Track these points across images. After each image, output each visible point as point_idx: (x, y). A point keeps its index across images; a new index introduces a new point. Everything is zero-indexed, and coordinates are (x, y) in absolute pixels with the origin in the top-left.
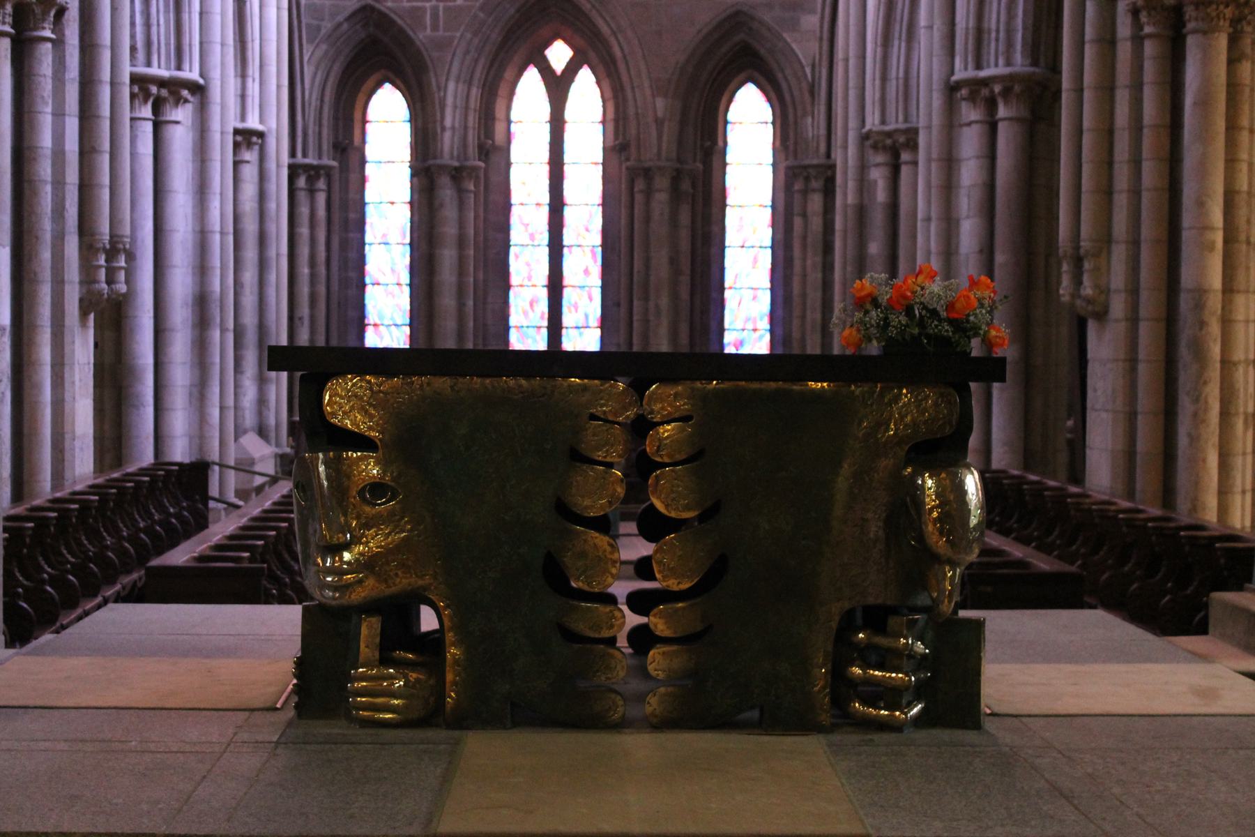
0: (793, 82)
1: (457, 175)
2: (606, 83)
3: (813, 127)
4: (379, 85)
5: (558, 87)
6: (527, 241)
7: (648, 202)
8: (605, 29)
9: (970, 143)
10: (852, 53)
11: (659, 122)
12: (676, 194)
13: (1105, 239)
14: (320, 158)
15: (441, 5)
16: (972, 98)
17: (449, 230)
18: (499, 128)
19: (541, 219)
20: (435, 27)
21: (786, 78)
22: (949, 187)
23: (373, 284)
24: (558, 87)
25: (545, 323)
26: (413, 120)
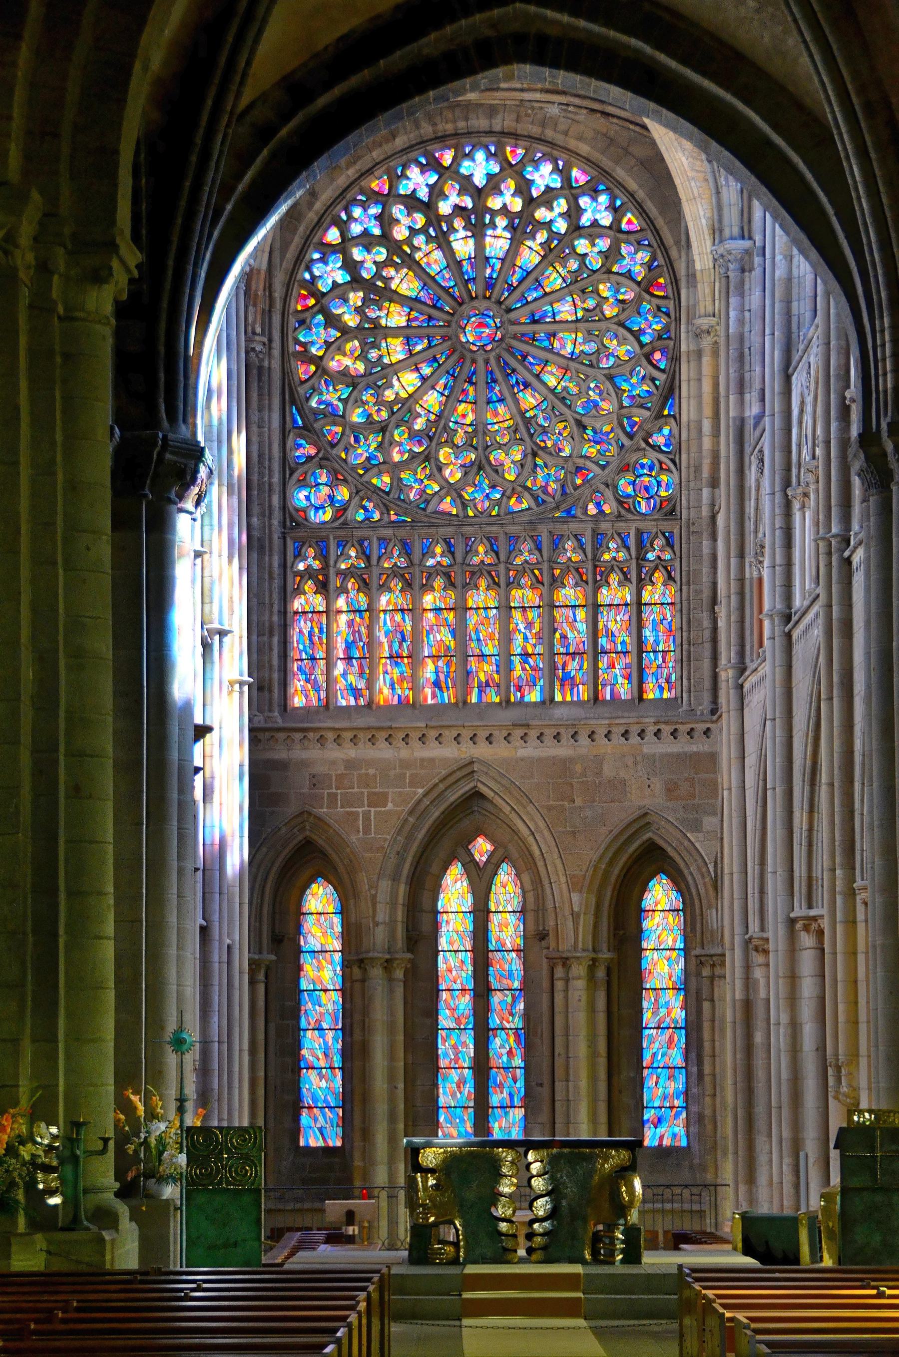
2: (526, 877)
4: (312, 880)
6: (453, 1025)
10: (735, 869)
11: (575, 916)
14: (260, 953)
15: (373, 810)
19: (465, 1003)
21: (691, 874)
23: (307, 1069)
25: (472, 1104)
26: (343, 912)
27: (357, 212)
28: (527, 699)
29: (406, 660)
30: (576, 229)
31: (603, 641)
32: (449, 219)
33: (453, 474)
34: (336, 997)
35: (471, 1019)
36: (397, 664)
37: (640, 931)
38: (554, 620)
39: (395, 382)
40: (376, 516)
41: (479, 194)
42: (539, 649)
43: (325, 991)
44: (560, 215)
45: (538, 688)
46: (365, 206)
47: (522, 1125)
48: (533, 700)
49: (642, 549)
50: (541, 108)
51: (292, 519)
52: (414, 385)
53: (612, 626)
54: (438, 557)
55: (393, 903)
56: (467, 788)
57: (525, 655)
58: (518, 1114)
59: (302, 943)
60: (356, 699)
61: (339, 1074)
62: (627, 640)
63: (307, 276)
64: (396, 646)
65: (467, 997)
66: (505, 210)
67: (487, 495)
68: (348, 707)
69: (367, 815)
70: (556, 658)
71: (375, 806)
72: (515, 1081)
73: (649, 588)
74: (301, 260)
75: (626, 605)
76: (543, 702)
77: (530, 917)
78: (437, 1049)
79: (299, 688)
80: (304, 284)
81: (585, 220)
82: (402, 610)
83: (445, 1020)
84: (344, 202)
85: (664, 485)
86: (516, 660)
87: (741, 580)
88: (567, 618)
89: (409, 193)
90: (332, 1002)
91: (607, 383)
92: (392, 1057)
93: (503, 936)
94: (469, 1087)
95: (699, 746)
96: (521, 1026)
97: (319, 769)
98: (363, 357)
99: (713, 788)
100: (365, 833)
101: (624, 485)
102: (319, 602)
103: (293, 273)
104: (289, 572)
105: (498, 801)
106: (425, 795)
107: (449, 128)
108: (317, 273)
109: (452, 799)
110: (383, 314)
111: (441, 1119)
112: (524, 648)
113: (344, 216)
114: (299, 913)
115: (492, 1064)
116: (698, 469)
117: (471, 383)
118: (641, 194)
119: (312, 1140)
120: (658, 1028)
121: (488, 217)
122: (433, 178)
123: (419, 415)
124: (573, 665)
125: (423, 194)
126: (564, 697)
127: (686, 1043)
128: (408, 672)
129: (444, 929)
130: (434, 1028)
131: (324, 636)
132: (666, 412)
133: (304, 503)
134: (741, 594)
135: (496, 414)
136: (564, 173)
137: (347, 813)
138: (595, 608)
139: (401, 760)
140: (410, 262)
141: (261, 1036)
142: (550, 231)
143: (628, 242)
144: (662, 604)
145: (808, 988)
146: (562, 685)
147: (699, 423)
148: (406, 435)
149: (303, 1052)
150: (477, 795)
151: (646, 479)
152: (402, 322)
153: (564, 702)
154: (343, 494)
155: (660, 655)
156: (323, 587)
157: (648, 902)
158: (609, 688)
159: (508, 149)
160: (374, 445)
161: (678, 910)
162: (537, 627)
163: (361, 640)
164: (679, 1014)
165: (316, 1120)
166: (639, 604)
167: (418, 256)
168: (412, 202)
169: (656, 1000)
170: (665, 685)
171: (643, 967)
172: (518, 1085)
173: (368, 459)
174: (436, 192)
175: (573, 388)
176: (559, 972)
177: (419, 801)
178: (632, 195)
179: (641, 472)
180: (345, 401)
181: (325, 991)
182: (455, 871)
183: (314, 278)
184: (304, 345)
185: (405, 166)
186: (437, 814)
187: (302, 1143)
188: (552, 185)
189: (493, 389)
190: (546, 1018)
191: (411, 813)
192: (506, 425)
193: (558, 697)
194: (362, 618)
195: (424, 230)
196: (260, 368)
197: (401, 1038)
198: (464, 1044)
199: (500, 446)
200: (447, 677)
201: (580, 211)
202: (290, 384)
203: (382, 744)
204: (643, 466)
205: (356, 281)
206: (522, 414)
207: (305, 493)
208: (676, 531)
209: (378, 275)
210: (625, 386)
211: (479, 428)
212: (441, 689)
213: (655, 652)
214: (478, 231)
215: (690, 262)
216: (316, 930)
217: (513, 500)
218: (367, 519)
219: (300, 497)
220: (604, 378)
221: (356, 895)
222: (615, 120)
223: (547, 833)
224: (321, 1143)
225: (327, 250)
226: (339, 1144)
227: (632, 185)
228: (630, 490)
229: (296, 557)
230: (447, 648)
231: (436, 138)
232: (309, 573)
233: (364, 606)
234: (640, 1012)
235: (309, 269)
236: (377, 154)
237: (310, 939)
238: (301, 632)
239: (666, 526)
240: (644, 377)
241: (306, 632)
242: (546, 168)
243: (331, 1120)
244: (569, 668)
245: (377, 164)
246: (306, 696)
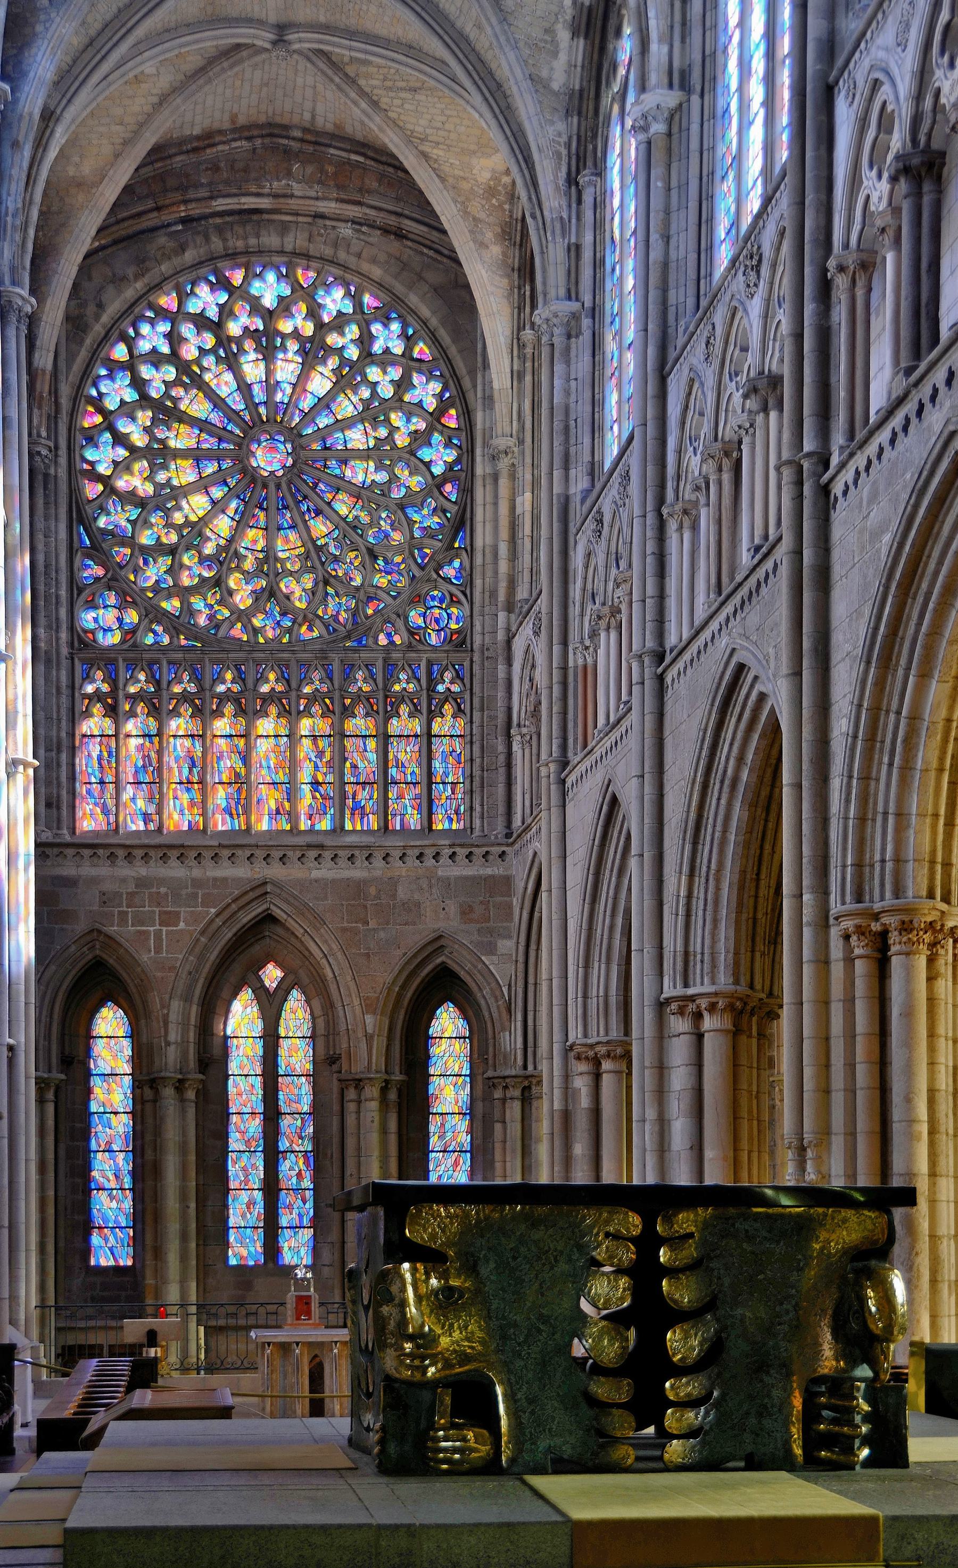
0: (491, 1001)
2: (316, 1003)
3: (511, 1040)
4: (101, 1004)
6: (243, 1148)
19: (255, 1126)
23: (98, 1190)
25: (262, 1224)
27: (145, 329)
28: (317, 827)
29: (196, 786)
30: (367, 356)
31: (393, 771)
32: (239, 341)
33: (243, 600)
34: (125, 1118)
35: (261, 1142)
36: (188, 790)
37: (428, 1057)
38: (343, 749)
39: (184, 503)
40: (166, 640)
41: (269, 315)
42: (330, 778)
43: (116, 1113)
44: (352, 341)
45: (328, 816)
46: (152, 322)
47: (311, 1244)
48: (324, 828)
50: (334, 227)
51: (81, 641)
52: (204, 509)
53: (402, 756)
54: (227, 683)
55: (185, 1025)
56: (260, 910)
57: (315, 784)
58: (307, 1234)
59: (92, 1066)
60: (145, 824)
61: (129, 1194)
62: (417, 771)
63: (94, 393)
64: (186, 772)
65: (257, 1121)
66: (296, 334)
67: (278, 623)
68: (138, 832)
69: (158, 934)
70: (347, 788)
71: (168, 925)
72: (304, 1202)
73: (439, 719)
74: (87, 376)
75: (416, 736)
76: (333, 831)
77: (321, 1042)
78: (227, 1171)
79: (88, 812)
80: (91, 400)
81: (377, 348)
82: (192, 736)
83: (235, 1142)
84: (131, 318)
85: (454, 617)
86: (307, 789)
88: (357, 747)
89: (198, 312)
90: (122, 1124)
91: (399, 512)
92: (184, 1177)
93: (292, 1061)
94: (260, 1208)
96: (310, 1149)
98: (150, 478)
100: (157, 952)
101: (415, 617)
102: (108, 725)
103: (79, 388)
104: (77, 695)
105: (291, 923)
106: (218, 915)
107: (240, 244)
108: (103, 390)
109: (245, 920)
110: (171, 435)
111: (232, 1239)
112: (314, 777)
113: (131, 332)
114: (89, 1037)
115: (282, 1185)
117: (261, 508)
118: (434, 322)
119: (102, 1259)
120: (444, 1151)
121: (279, 340)
122: (223, 297)
123: (209, 539)
124: (363, 795)
125: (213, 313)
126: (354, 825)
127: (471, 1166)
128: (198, 798)
129: (234, 1053)
130: (225, 1151)
131: (113, 760)
132: (457, 545)
133: (91, 626)
135: (287, 540)
136: (356, 299)
137: (139, 931)
138: (385, 739)
139: (193, 880)
140: (198, 383)
141: (51, 1156)
142: (341, 357)
143: (420, 372)
144: (452, 736)
146: (353, 814)
148: (196, 560)
149: (93, 1174)
150: (269, 919)
151: (437, 611)
152: (192, 443)
153: (354, 831)
154: (132, 617)
155: (449, 787)
156: (112, 711)
157: (435, 1029)
158: (398, 818)
159: (300, 272)
160: (164, 568)
161: (465, 1038)
162: (328, 756)
163: (151, 765)
164: (465, 1139)
165: (106, 1240)
166: (429, 735)
167: (207, 377)
168: (201, 321)
169: (443, 1125)
170: (454, 817)
171: (431, 1092)
172: (307, 1206)
173: (157, 582)
174: (226, 311)
175: (364, 518)
176: (351, 1094)
177: (212, 921)
178: (425, 324)
179: (432, 604)
180: (133, 523)
181: (116, 1113)
182: (246, 995)
183: (101, 395)
184: (92, 464)
185: (194, 284)
186: (230, 935)
187: (93, 1263)
188: (344, 311)
189: (284, 515)
190: (336, 1140)
191: (203, 932)
192: (297, 552)
193: (348, 826)
194: (151, 742)
195: (213, 351)
197: (192, 1158)
198: (254, 1166)
199: (291, 573)
200: (238, 803)
201: (372, 338)
202: (77, 502)
204: (433, 598)
205: (144, 400)
206: (313, 542)
207: (92, 614)
208: (467, 664)
209: (167, 394)
210: (416, 517)
211: (269, 556)
212: (231, 815)
213: (444, 783)
214: (268, 353)
216: (105, 1054)
217: (304, 628)
218: (156, 643)
219: (87, 619)
220: (395, 508)
221: (148, 1015)
222: (409, 243)
223: (340, 955)
224: (112, 1263)
225: (114, 367)
226: (130, 1263)
227: (425, 312)
228: (420, 621)
229: (84, 679)
230: (237, 775)
231: (227, 255)
232: (98, 696)
233: (154, 732)
234: (426, 1136)
235: (95, 385)
236: (165, 268)
237: (100, 1062)
238: (89, 755)
239: (454, 656)
240: (435, 510)
241: (95, 755)
242: (338, 293)
243: (122, 1240)
244: (359, 797)
245: (166, 279)
246: (96, 820)
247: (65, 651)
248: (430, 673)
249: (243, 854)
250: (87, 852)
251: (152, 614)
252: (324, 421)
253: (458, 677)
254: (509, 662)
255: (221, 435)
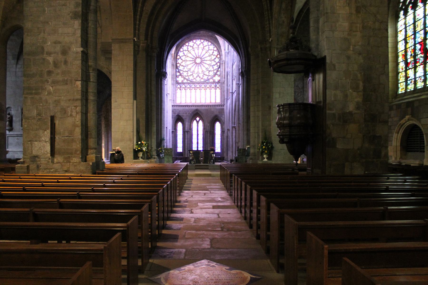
1: (187, 132)
5: (198, 122)
7: (207, 134)
8: (203, 117)
9: (234, 131)
11: (208, 126)
12: (210, 134)
13: (239, 141)
16: (234, 128)
17: (186, 138)
18: (192, 127)
20: (185, 117)
22: (232, 135)
24: (198, 122)
49: (216, 86)
74: (178, 53)
87: (227, 89)
95: (222, 107)
97: (180, 110)
99: (224, 112)
116: (222, 76)
134: (227, 90)
145: (234, 134)
147: (223, 71)
176: (206, 133)
196: (173, 65)
203: (187, 107)
215: (222, 53)
219: (178, 79)
247: (175, 83)
248: (216, 84)
249: (194, 106)
250: (177, 106)
251: (185, 78)
252: (204, 57)
253: (219, 85)
254: (224, 84)
255: (193, 59)
